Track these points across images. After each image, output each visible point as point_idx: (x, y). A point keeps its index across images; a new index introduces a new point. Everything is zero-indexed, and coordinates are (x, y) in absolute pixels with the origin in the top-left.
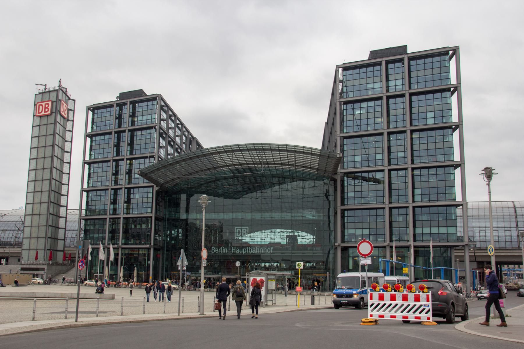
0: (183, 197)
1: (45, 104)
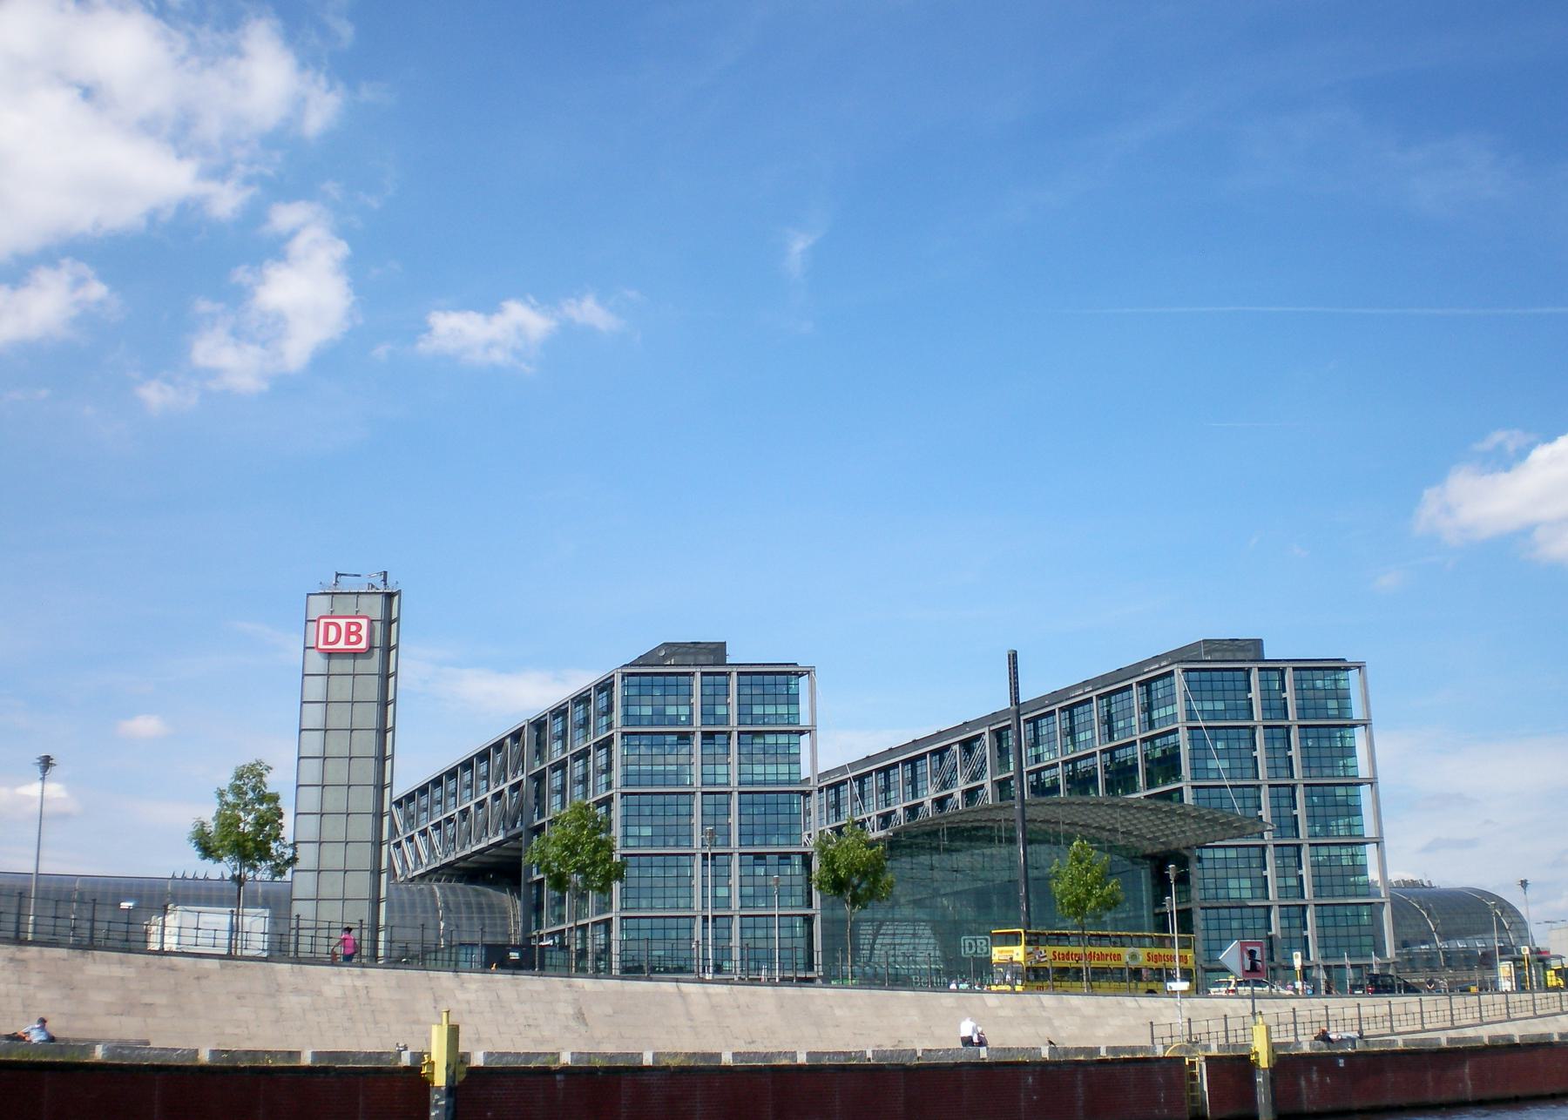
1: (349, 625)
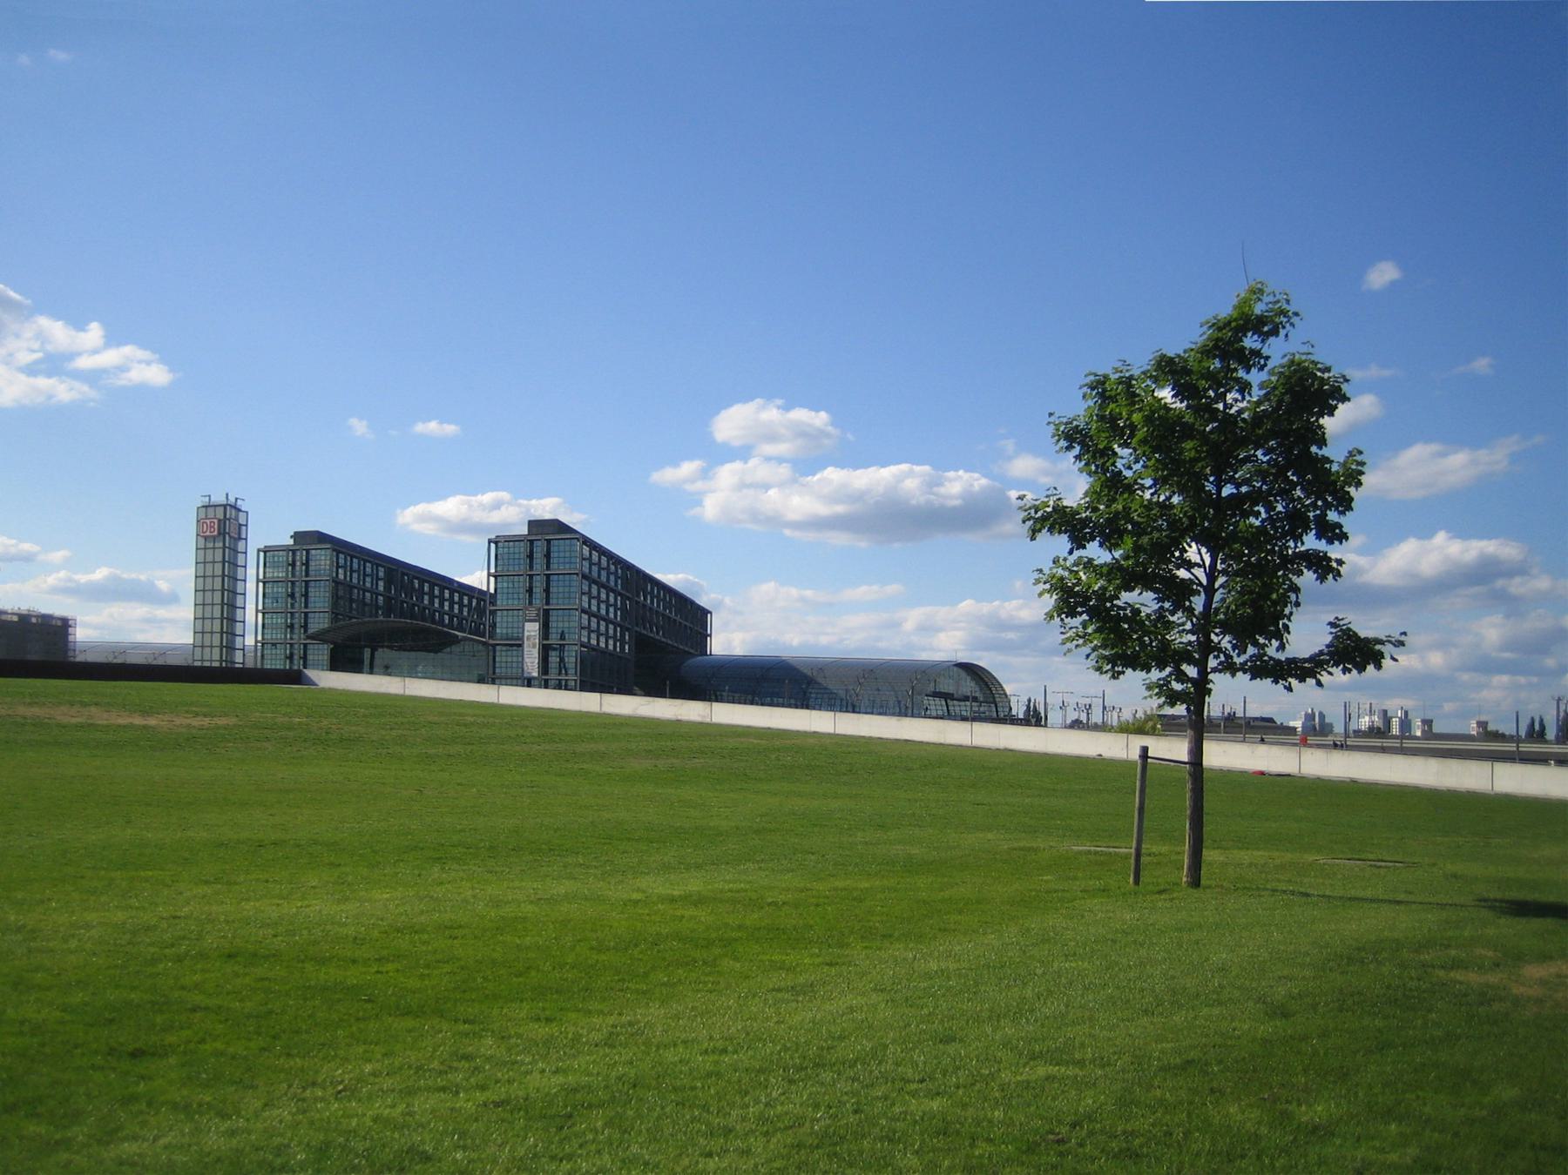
0: (367, 653)
1: (211, 522)
